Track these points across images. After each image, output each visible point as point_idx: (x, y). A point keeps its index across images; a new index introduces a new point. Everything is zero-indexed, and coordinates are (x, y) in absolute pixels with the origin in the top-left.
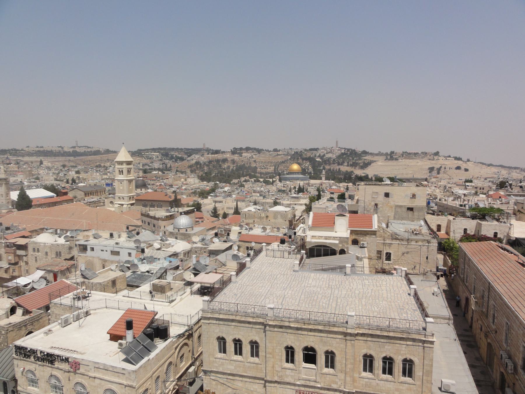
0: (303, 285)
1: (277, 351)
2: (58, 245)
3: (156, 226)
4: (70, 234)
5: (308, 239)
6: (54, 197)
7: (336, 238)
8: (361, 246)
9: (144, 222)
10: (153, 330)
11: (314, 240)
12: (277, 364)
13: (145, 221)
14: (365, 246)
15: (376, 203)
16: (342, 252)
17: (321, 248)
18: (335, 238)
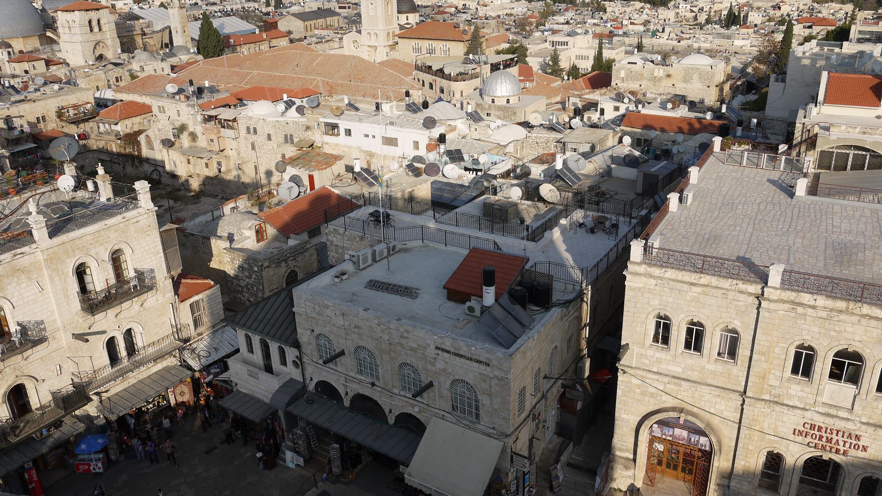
0: (823, 228)
1: (777, 350)
2: (287, 123)
9: (421, 82)
10: (525, 290)
12: (774, 374)
13: (423, 81)
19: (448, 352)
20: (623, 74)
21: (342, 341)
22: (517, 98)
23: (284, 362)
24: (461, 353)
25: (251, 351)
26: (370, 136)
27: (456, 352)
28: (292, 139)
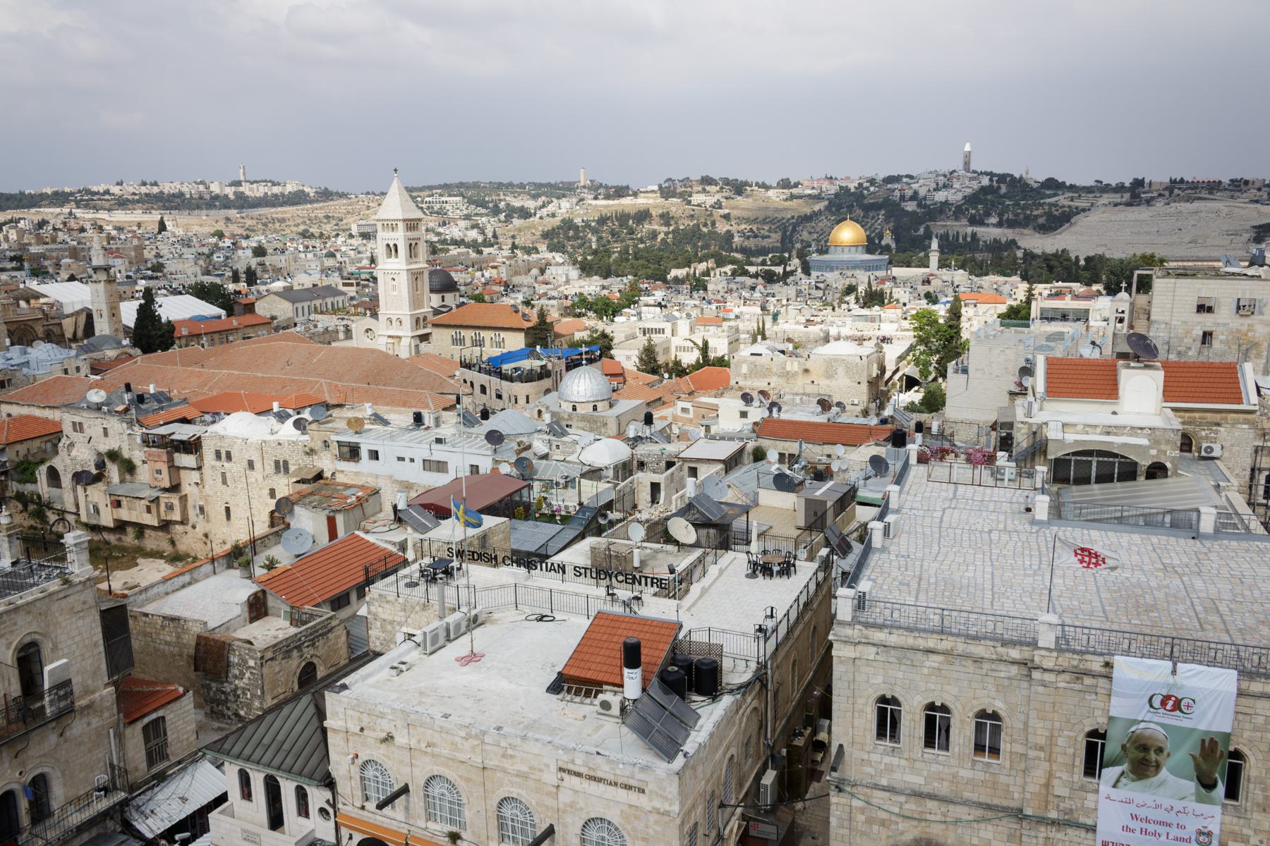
1: (1061, 741)
2: (279, 444)
3: (505, 396)
4: (311, 413)
5: (1052, 433)
6: (220, 317)
7: (1139, 431)
8: (1203, 454)
9: (469, 384)
10: (683, 672)
11: (1070, 437)
12: (1060, 778)
13: (472, 384)
14: (1213, 454)
15: (1208, 329)
16: (1157, 471)
17: (1090, 459)
18: (1135, 430)
19: (578, 775)
20: (744, 369)
21: (407, 770)
22: (606, 403)
23: (303, 810)
24: (599, 774)
25: (247, 794)
26: (407, 460)
27: (592, 773)
28: (286, 470)
